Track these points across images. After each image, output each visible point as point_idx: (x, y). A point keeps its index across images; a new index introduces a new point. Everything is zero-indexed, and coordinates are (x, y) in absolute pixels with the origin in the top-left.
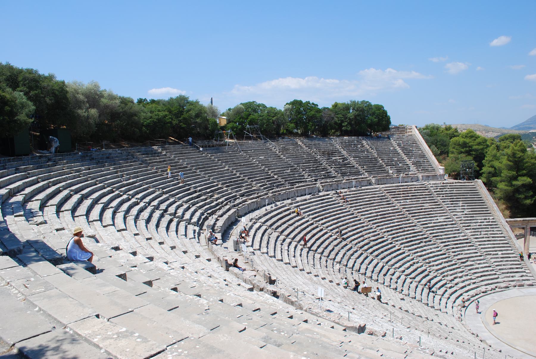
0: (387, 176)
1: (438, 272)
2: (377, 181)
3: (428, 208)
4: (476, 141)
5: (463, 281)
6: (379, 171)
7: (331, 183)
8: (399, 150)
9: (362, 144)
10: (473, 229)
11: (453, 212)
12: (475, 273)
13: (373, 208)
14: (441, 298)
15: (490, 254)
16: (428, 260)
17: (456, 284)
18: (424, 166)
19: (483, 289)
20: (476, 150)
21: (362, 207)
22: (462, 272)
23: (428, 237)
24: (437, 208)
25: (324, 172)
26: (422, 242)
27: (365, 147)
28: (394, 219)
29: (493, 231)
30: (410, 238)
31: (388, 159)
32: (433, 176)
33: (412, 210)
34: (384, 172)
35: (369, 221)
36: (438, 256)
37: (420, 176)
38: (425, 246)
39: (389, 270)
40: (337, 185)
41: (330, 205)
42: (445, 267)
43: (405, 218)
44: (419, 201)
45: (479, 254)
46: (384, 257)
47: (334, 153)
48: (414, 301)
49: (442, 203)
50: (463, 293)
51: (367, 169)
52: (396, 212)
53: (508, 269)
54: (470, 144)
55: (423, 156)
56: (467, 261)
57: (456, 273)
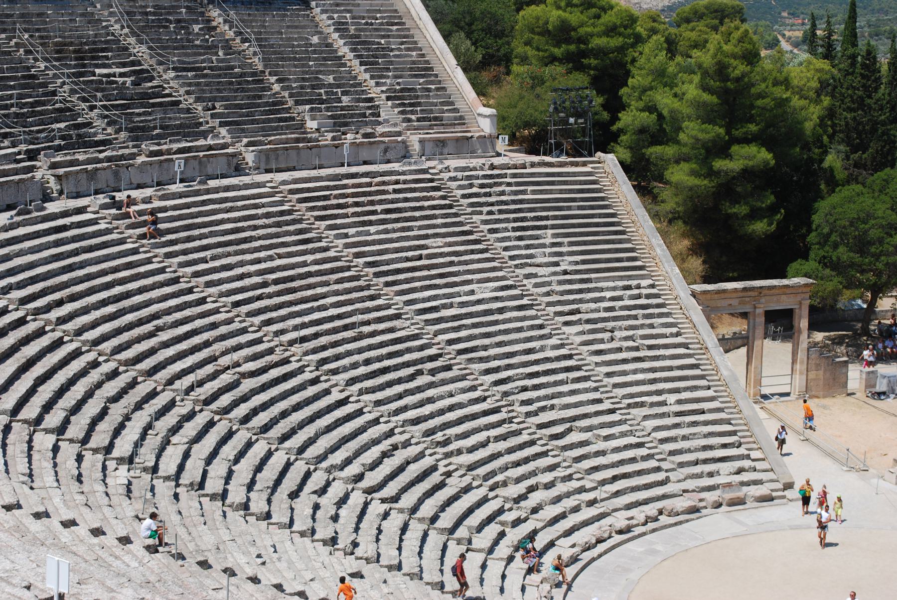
0: (297, 140)
1: (475, 472)
2: (263, 158)
3: (442, 255)
4: (602, 20)
5: (557, 500)
6: (269, 121)
7: (90, 167)
8: (343, 49)
9: (209, 21)
10: (588, 321)
11: (522, 266)
12: (596, 469)
13: (248, 257)
14: (486, 560)
15: (642, 405)
16: (440, 434)
17: (535, 511)
18: (427, 104)
19: (620, 520)
20: (600, 53)
21: (208, 254)
22: (552, 468)
23: (440, 355)
24: (472, 252)
25: (62, 125)
26: (420, 373)
27: (218, 30)
28: (324, 296)
29: (652, 326)
30: (380, 359)
31: (304, 80)
32: (457, 140)
33: (388, 263)
34: (288, 127)
35: (237, 304)
36: (474, 417)
37: (414, 140)
38: (431, 385)
39: (308, 475)
40: (116, 174)
41: (91, 249)
42: (499, 455)
43: (361, 289)
44: (410, 229)
45: (606, 405)
46: (292, 432)
47: (103, 50)
48: (396, 578)
49: (489, 236)
50: (558, 538)
51: (228, 115)
52: (333, 271)
53: (696, 450)
54: (582, 31)
55: (425, 69)
56: (570, 430)
57: (533, 474)
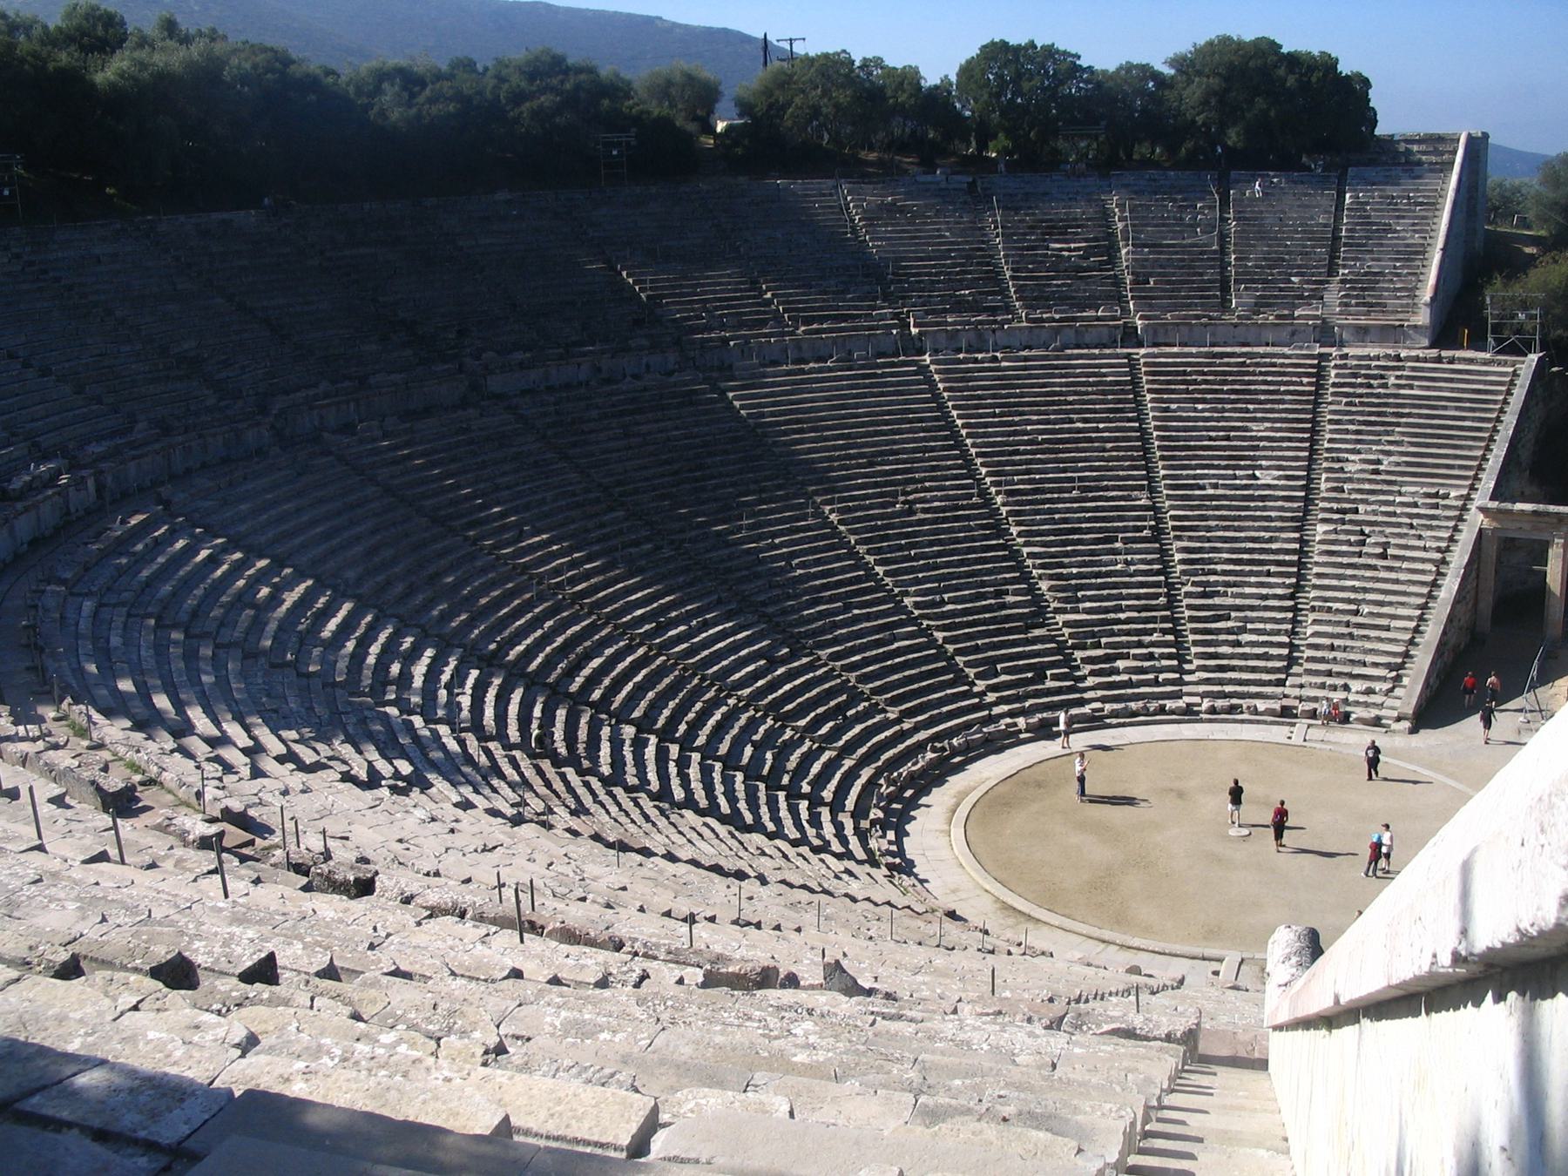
2: (1151, 332)
24: (1290, 440)
47: (1078, 227)
